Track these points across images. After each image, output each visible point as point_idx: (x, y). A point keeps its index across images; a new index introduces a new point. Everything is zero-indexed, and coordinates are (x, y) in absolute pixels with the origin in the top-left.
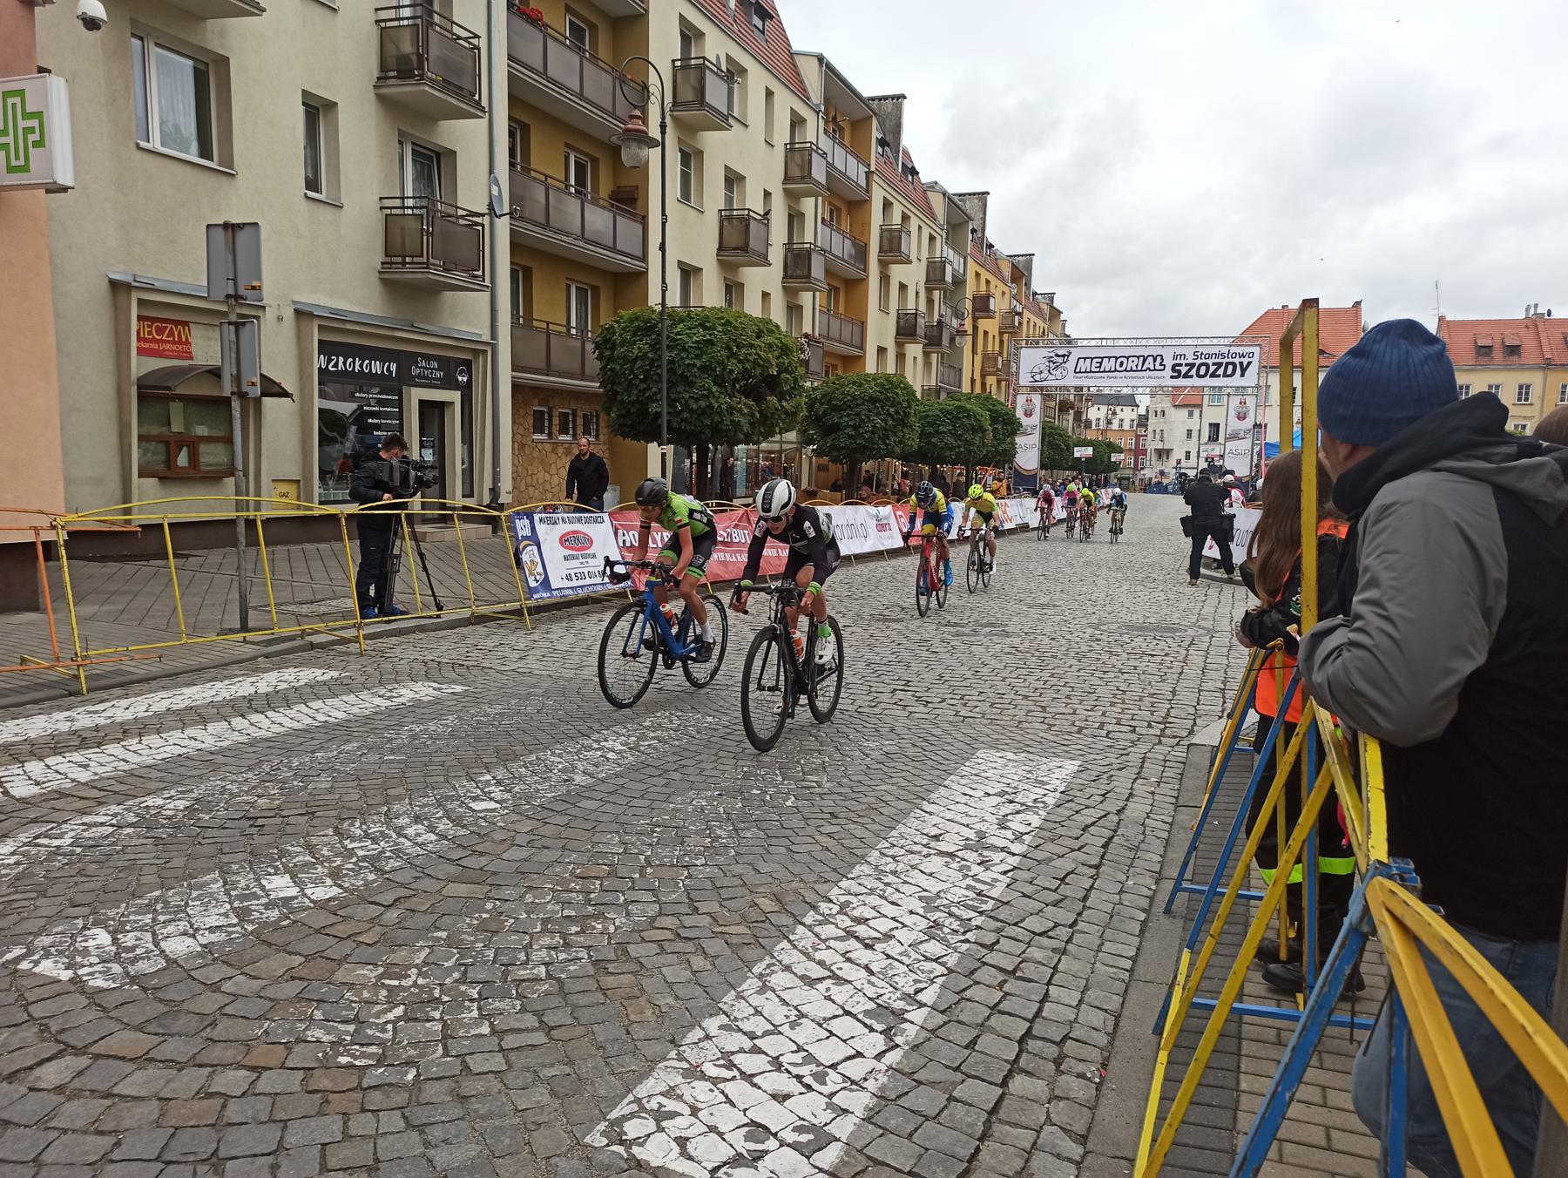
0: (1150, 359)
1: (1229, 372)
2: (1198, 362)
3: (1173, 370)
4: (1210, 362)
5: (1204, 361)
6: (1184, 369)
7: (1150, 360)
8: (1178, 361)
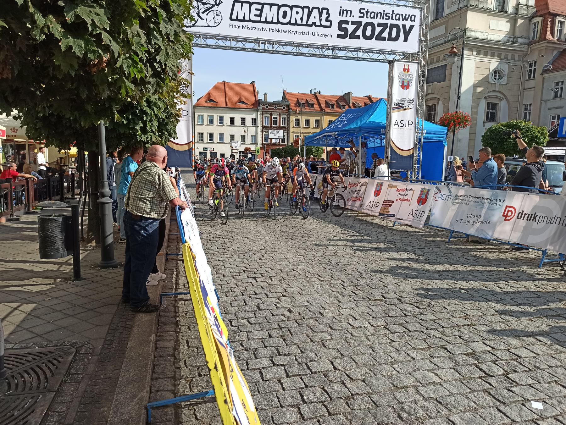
0: (315, 12)
1: (394, 35)
2: (364, 21)
3: (340, 28)
4: (376, 21)
5: (370, 20)
6: (351, 28)
7: (315, 12)
8: (344, 18)
